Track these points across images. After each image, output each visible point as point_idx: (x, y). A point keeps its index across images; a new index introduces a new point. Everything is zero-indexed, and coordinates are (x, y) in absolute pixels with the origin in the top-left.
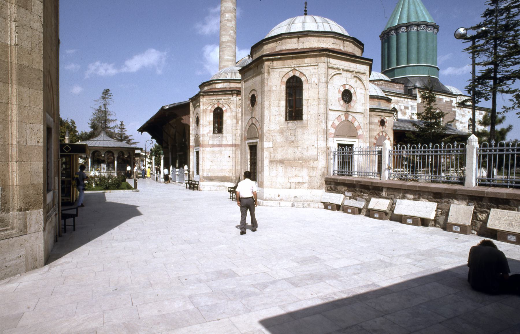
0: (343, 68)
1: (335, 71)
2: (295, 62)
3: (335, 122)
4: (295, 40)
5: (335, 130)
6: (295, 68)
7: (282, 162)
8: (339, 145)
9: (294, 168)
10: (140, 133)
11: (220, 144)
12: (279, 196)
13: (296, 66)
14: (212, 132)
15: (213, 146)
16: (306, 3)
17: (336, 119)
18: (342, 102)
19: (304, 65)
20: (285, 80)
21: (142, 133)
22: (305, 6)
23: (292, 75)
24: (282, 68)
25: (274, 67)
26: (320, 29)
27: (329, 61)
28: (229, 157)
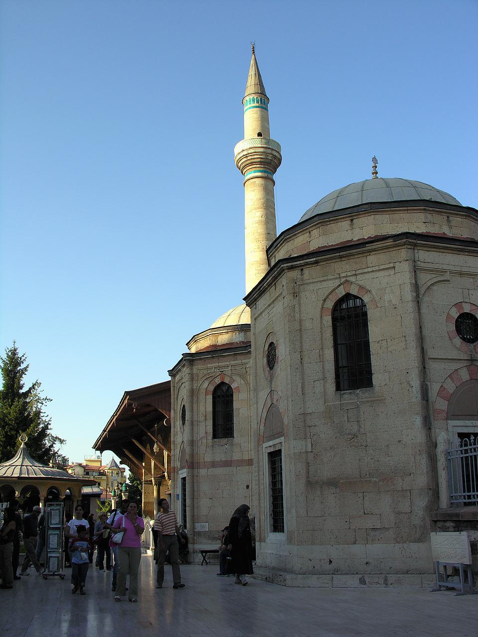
0: (452, 268)
1: (434, 276)
2: (348, 267)
3: (445, 386)
4: (345, 224)
5: (447, 402)
6: (348, 278)
7: (332, 483)
8: (461, 435)
9: (360, 495)
10: (99, 452)
11: (226, 461)
12: (331, 562)
13: (349, 274)
14: (210, 436)
15: (214, 464)
16: (375, 160)
17: (449, 379)
18: (458, 341)
19: (366, 270)
20: (330, 305)
21: (101, 453)
22: (373, 165)
23: (344, 293)
24: (321, 281)
25: (305, 282)
26: (394, 198)
27: (417, 255)
28: (248, 487)
